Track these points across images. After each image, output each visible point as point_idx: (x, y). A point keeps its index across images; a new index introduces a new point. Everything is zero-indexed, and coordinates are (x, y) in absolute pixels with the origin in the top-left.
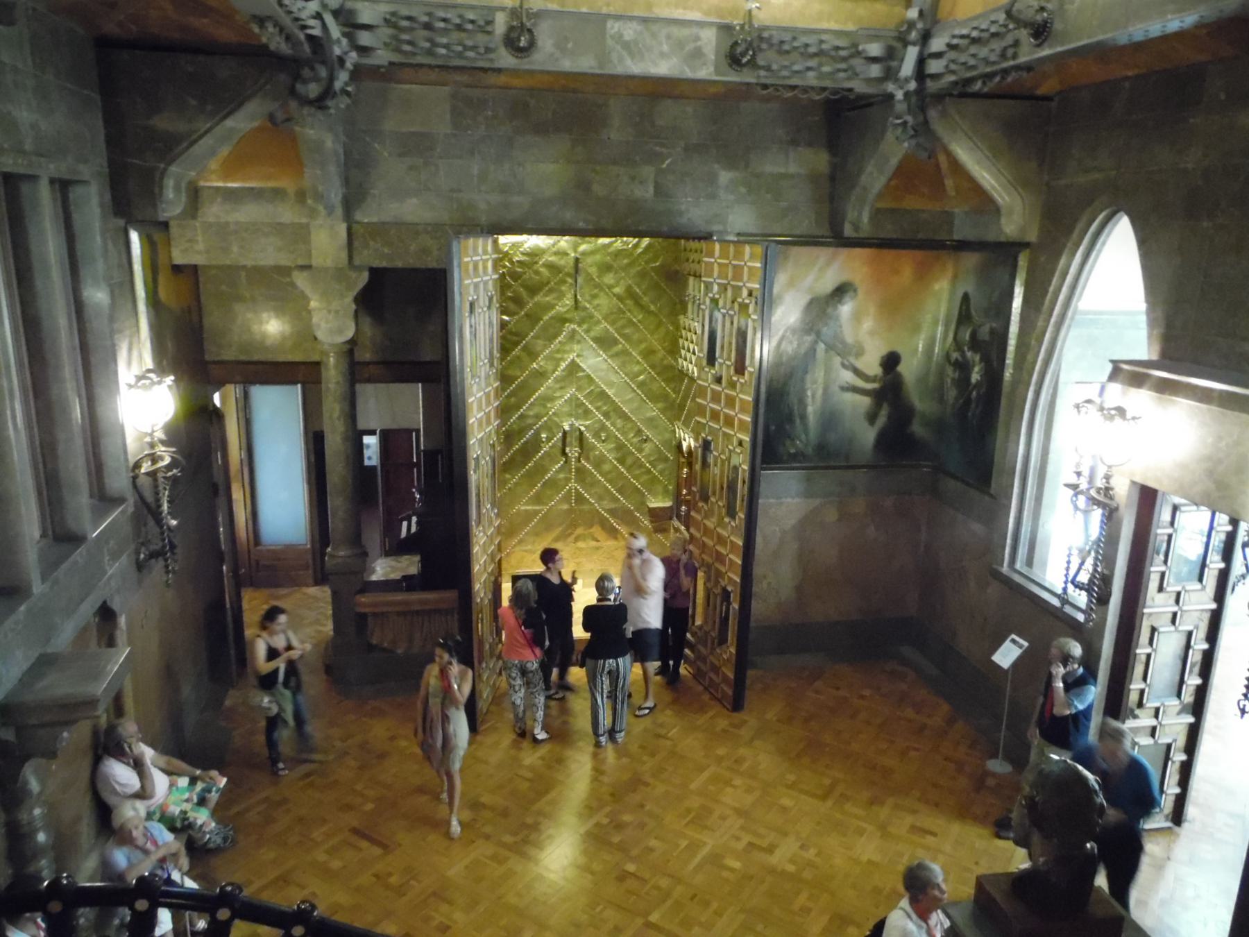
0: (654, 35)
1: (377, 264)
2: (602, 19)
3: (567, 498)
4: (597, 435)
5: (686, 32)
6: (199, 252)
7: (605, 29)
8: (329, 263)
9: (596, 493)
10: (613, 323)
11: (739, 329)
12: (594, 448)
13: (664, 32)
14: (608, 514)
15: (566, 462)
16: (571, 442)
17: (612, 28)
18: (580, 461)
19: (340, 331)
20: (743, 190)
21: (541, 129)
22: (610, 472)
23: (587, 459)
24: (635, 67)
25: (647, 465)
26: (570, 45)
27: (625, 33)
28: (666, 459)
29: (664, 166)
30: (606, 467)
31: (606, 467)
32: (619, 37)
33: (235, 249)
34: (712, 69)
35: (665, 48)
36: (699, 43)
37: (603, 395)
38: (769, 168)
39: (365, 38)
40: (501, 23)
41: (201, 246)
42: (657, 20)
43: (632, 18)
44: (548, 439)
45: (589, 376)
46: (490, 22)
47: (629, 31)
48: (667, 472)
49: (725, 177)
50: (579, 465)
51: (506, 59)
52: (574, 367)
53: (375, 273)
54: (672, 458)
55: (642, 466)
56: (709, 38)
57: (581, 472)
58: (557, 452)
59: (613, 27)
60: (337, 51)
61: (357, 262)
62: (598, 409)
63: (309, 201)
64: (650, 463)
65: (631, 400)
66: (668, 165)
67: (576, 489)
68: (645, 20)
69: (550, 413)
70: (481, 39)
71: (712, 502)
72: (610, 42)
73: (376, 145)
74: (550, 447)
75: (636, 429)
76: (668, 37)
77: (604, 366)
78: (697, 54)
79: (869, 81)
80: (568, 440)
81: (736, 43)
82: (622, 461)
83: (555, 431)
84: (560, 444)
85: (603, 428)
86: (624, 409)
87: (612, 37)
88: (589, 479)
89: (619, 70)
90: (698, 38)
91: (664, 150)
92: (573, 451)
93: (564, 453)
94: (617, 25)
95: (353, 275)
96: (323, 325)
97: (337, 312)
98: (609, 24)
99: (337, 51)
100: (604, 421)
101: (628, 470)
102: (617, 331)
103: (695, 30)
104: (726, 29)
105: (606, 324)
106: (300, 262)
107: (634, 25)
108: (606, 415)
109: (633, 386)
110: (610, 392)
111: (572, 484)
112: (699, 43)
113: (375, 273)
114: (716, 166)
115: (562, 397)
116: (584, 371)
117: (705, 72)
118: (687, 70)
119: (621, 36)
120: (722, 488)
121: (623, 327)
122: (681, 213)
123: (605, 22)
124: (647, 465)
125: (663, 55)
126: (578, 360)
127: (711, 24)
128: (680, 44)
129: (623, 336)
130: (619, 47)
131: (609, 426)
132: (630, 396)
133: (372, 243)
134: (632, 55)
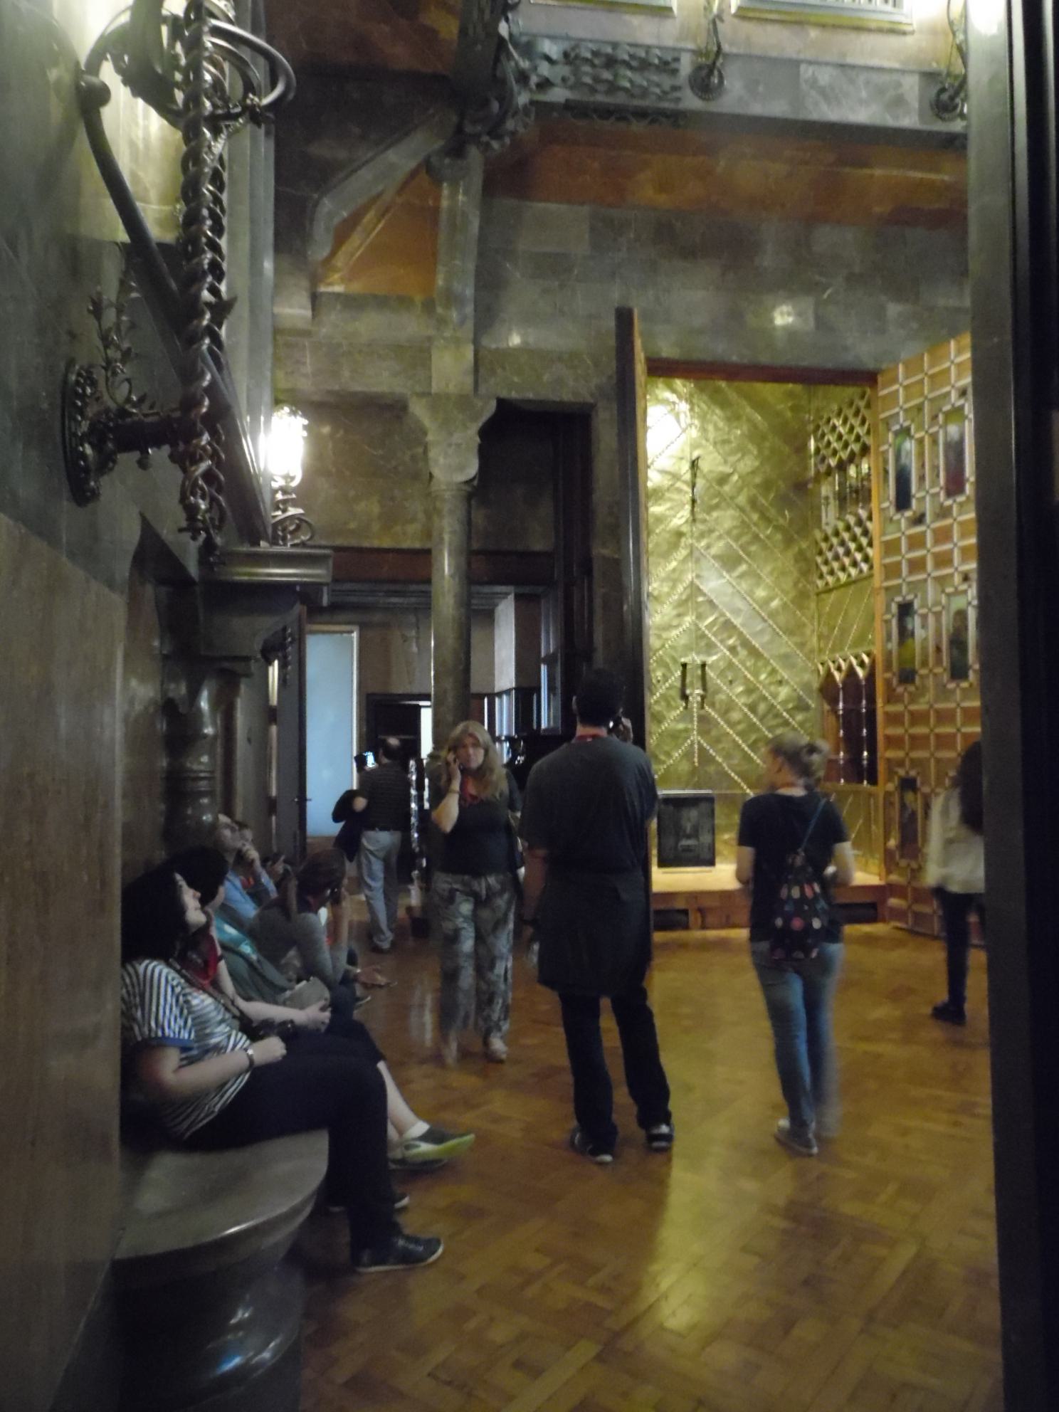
0: (852, 81)
1: (504, 394)
2: (795, 63)
3: (688, 755)
4: (721, 674)
5: (886, 78)
6: (305, 376)
7: (799, 72)
8: (452, 389)
9: (723, 749)
10: (736, 539)
11: (948, 446)
12: (719, 691)
13: (862, 77)
14: (739, 776)
15: (686, 708)
16: (692, 683)
18: (702, 708)
19: (461, 468)
20: (915, 325)
21: (690, 253)
22: (739, 722)
23: (712, 705)
24: (832, 114)
25: (785, 714)
26: (761, 89)
28: (806, 708)
29: (825, 296)
30: (735, 716)
31: (735, 716)
32: (813, 83)
33: (346, 373)
35: (864, 94)
37: (728, 626)
38: (941, 302)
40: (686, 66)
41: (308, 369)
42: (853, 67)
43: (827, 64)
44: (666, 678)
45: (711, 602)
46: (677, 60)
47: (825, 76)
48: (808, 725)
49: (894, 309)
50: (702, 712)
51: (691, 102)
52: (694, 590)
53: (501, 402)
54: (813, 706)
55: (778, 715)
56: (911, 87)
57: (704, 719)
58: (675, 693)
59: (806, 72)
61: (483, 389)
62: (722, 641)
63: (439, 310)
64: (788, 711)
65: (762, 632)
66: (829, 296)
67: (699, 742)
68: (842, 66)
69: (667, 646)
70: (667, 82)
71: (922, 677)
72: (804, 87)
73: (508, 265)
74: (667, 689)
75: (769, 668)
77: (730, 590)
78: (898, 102)
80: (688, 680)
81: (943, 90)
82: (753, 708)
83: (673, 668)
84: (678, 684)
85: (730, 665)
86: (754, 643)
87: (806, 81)
88: (714, 733)
89: (814, 116)
90: (899, 85)
91: (824, 280)
92: (695, 692)
93: (685, 697)
94: (811, 70)
95: (479, 404)
96: (441, 460)
97: (458, 445)
98: (803, 67)
100: (731, 657)
101: (761, 720)
102: (741, 547)
103: (895, 77)
104: (929, 76)
105: (729, 540)
106: (418, 389)
107: (829, 70)
108: (732, 649)
109: (763, 614)
110: (737, 622)
111: (695, 737)
113: (501, 402)
114: (883, 298)
115: (677, 627)
116: (704, 595)
117: (909, 120)
120: (938, 649)
121: (750, 543)
122: (846, 349)
123: (798, 66)
124: (785, 714)
125: (862, 102)
126: (697, 582)
127: (912, 72)
128: (880, 91)
129: (748, 554)
130: (813, 93)
131: (737, 663)
132: (759, 627)
133: (499, 371)
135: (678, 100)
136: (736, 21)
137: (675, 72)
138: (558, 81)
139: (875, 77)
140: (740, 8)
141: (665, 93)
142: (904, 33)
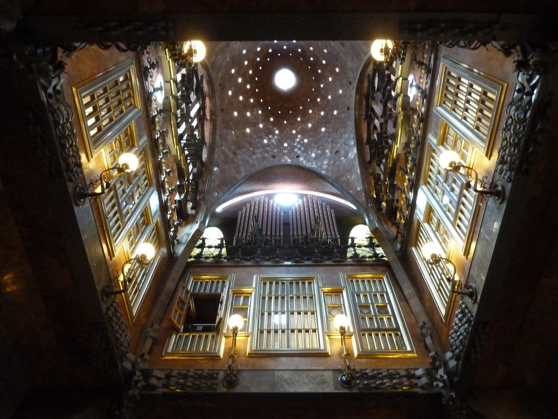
17: (278, 373)
27: (284, 375)
34: (333, 388)
35: (306, 380)
36: (324, 377)
39: (153, 381)
40: (221, 375)
46: (217, 374)
60: (136, 378)
76: (307, 376)
78: (324, 382)
79: (422, 387)
89: (282, 391)
90: (323, 375)
94: (280, 373)
99: (136, 378)
103: (320, 372)
112: (324, 377)
118: (318, 388)
119: (282, 376)
125: (305, 383)
134: (288, 384)
135: (216, 389)
136: (249, 358)
137: (216, 378)
138: (160, 386)
139: (312, 374)
140: (249, 354)
141: (209, 386)
142: (326, 357)
